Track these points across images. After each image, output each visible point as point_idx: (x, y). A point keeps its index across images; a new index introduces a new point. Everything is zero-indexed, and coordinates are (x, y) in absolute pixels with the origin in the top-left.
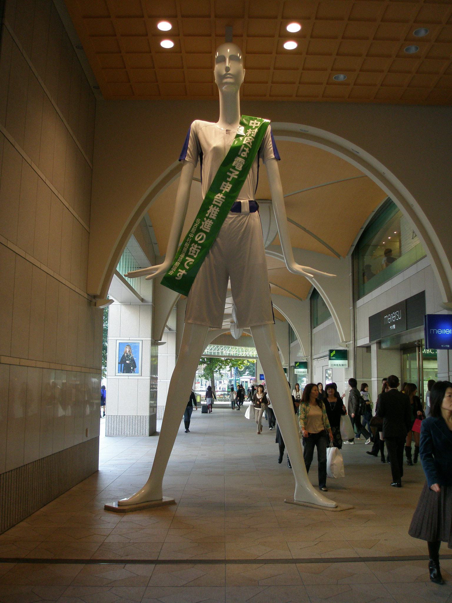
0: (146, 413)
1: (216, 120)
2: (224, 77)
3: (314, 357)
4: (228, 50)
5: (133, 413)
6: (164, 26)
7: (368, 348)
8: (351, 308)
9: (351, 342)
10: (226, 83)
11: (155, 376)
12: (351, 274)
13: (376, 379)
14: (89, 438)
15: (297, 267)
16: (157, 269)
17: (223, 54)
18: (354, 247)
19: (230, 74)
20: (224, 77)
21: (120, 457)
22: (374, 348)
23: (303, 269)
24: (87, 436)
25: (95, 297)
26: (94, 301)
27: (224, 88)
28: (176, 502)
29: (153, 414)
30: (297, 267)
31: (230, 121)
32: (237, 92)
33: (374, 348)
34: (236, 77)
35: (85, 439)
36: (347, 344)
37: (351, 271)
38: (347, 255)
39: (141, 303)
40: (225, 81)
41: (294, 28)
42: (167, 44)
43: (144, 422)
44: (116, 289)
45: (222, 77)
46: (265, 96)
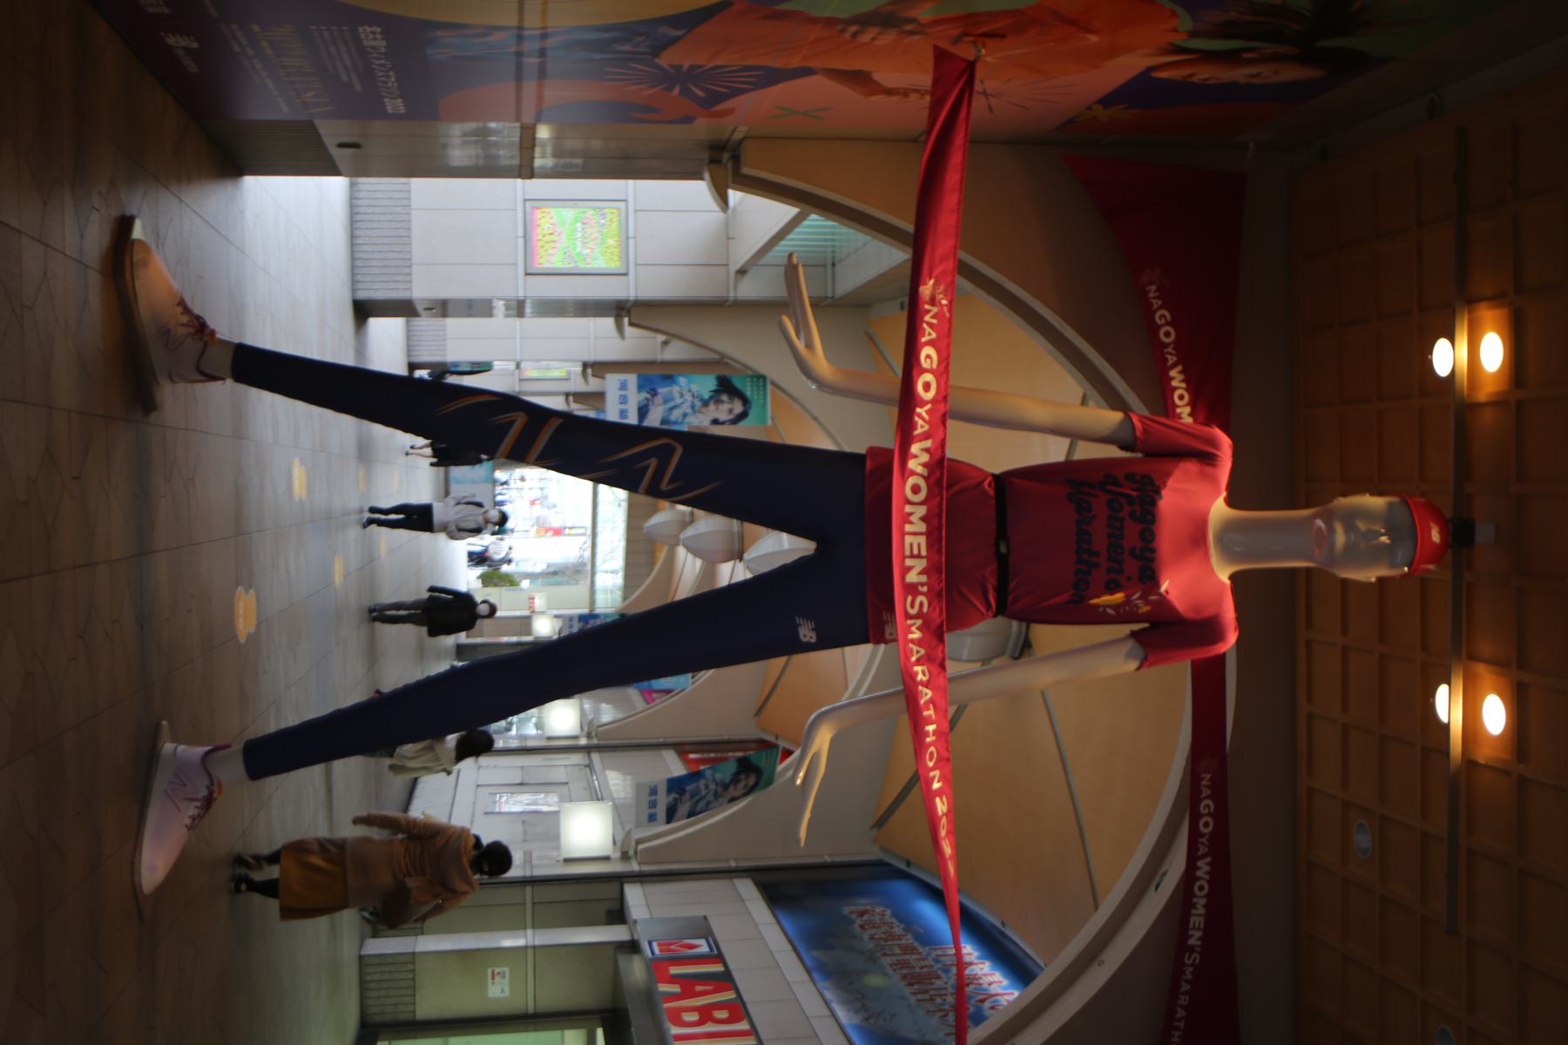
0: (421, 290)
1: (1230, 502)
3: (595, 757)
5: (418, 254)
6: (1493, 352)
7: (618, 915)
8: (733, 864)
9: (635, 867)
10: (1331, 530)
11: (528, 309)
12: (828, 859)
13: (530, 943)
14: (335, 152)
15: (823, 739)
16: (809, 346)
18: (903, 866)
21: (282, 244)
22: (617, 933)
23: (816, 756)
24: (341, 145)
25: (736, 159)
26: (726, 156)
27: (1320, 523)
28: (154, 416)
29: (420, 308)
30: (823, 739)
32: (1310, 559)
33: (617, 933)
35: (330, 143)
36: (631, 853)
37: (837, 859)
38: (885, 850)
39: (734, 267)
40: (1339, 530)
41: (1495, 715)
42: (1445, 357)
43: (394, 285)
44: (761, 216)
46: (1309, 626)
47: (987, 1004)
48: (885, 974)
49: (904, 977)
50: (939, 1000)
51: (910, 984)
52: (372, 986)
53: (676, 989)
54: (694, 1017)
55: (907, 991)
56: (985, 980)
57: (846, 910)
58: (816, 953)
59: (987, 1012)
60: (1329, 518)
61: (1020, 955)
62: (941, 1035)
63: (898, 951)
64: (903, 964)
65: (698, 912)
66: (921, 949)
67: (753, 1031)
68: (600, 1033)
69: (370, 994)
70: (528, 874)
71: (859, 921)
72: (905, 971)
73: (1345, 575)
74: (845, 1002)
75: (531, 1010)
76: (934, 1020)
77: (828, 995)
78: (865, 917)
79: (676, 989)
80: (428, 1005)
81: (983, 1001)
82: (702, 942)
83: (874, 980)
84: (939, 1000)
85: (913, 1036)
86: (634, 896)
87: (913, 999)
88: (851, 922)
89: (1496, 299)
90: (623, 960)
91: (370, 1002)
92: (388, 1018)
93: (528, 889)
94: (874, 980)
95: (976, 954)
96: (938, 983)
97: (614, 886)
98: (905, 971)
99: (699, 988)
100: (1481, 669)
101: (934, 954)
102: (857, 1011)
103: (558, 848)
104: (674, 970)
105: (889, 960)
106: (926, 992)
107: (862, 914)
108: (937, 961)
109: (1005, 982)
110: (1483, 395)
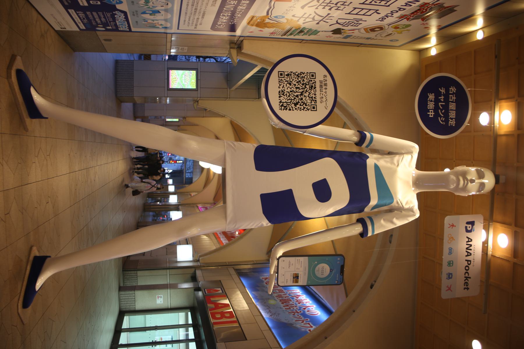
1: (419, 167)
2: (465, 178)
4: (489, 181)
9: (199, 264)
10: (459, 180)
14: (103, 42)
17: (486, 176)
19: (467, 183)
20: (465, 178)
24: (105, 40)
26: (236, 47)
31: (417, 182)
32: (447, 189)
34: (465, 188)
42: (484, 119)
45: (464, 174)
47: (306, 310)
48: (275, 300)
49: (281, 301)
50: (292, 309)
51: (283, 303)
52: (123, 300)
53: (212, 306)
54: (218, 316)
55: (282, 305)
56: (305, 301)
57: (261, 278)
58: (253, 293)
59: (307, 313)
60: (457, 174)
61: (314, 293)
62: (294, 321)
63: (278, 291)
64: (279, 296)
65: (217, 278)
66: (284, 291)
67: (238, 321)
68: (189, 313)
69: (122, 303)
70: (168, 266)
71: (265, 281)
72: (281, 299)
73: (458, 194)
74: (264, 310)
75: (169, 307)
76: (291, 316)
77: (259, 307)
78: (267, 280)
79: (212, 306)
80: (138, 307)
81: (305, 309)
82: (220, 289)
83: (272, 302)
84: (292, 309)
85: (286, 322)
86: (199, 273)
87: (284, 308)
88: (263, 282)
89: (508, 98)
90: (196, 292)
91: (122, 305)
92: (127, 310)
93: (168, 270)
94: (272, 302)
95: (301, 292)
96: (291, 302)
97: (193, 270)
98: (281, 299)
99: (220, 305)
100: (499, 226)
101: (288, 292)
102: (268, 313)
103: (176, 257)
104: (212, 299)
105: (276, 295)
106: (288, 306)
107: (266, 279)
108: (290, 295)
109: (311, 302)
110: (503, 131)
